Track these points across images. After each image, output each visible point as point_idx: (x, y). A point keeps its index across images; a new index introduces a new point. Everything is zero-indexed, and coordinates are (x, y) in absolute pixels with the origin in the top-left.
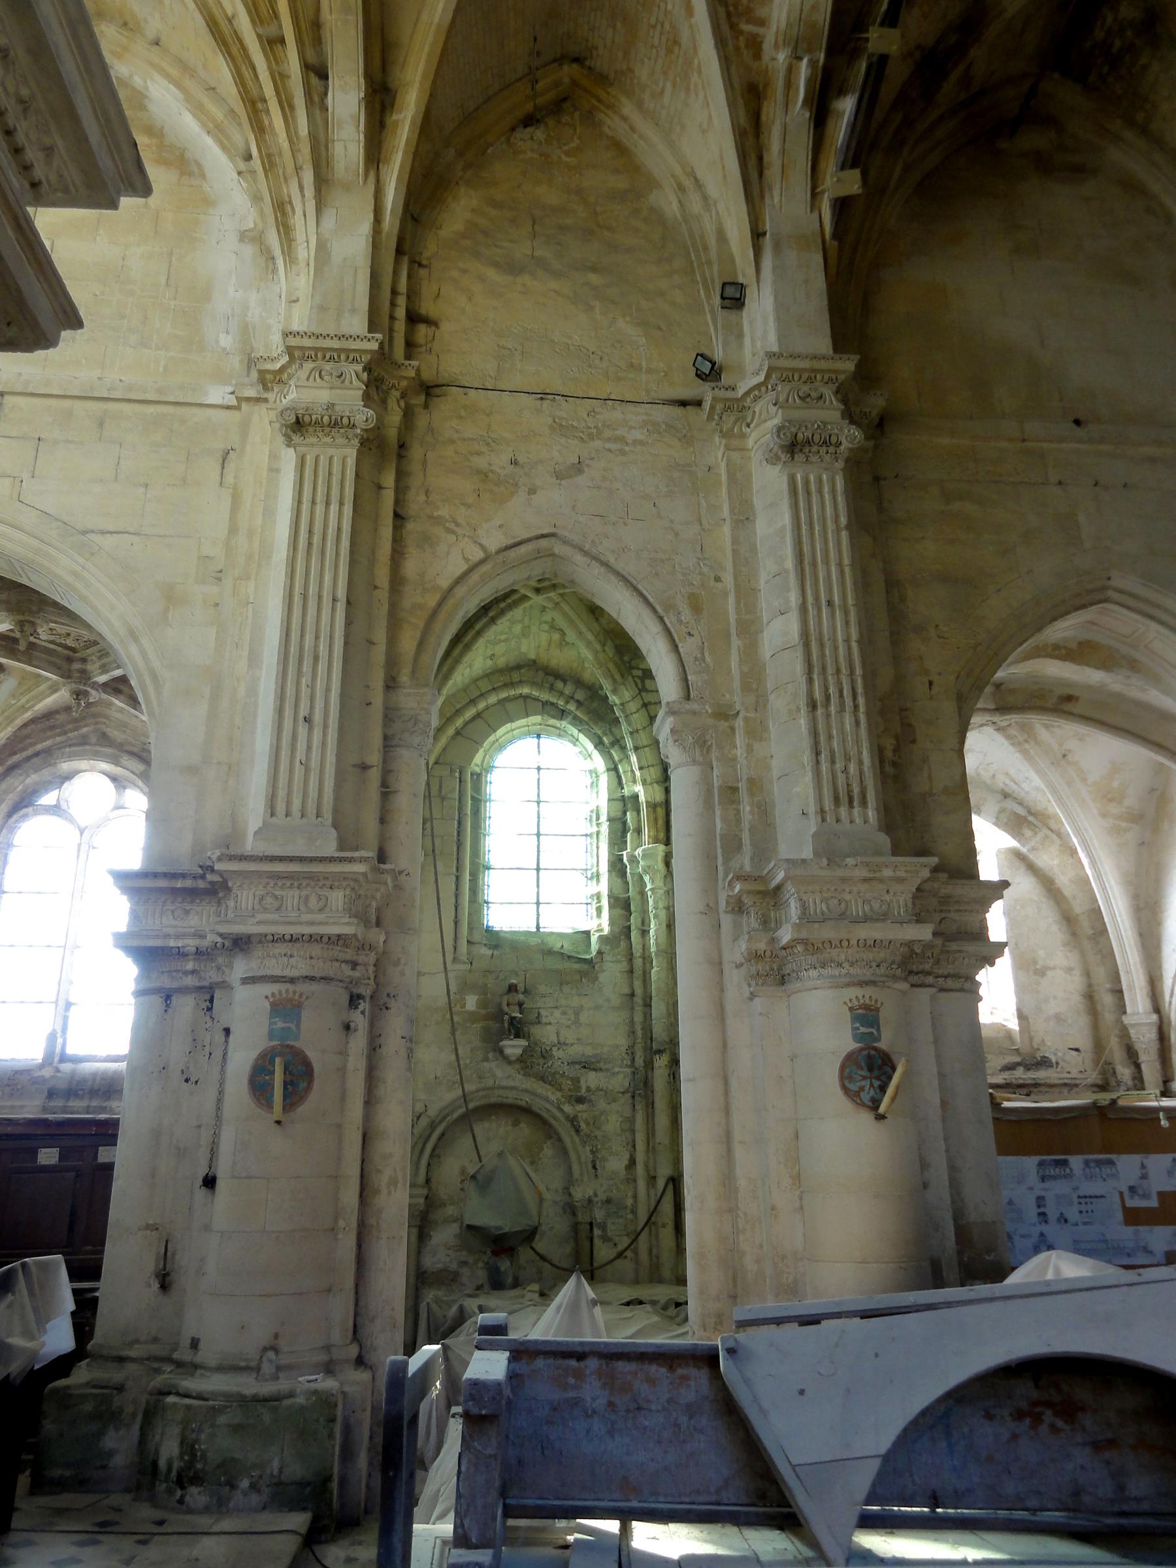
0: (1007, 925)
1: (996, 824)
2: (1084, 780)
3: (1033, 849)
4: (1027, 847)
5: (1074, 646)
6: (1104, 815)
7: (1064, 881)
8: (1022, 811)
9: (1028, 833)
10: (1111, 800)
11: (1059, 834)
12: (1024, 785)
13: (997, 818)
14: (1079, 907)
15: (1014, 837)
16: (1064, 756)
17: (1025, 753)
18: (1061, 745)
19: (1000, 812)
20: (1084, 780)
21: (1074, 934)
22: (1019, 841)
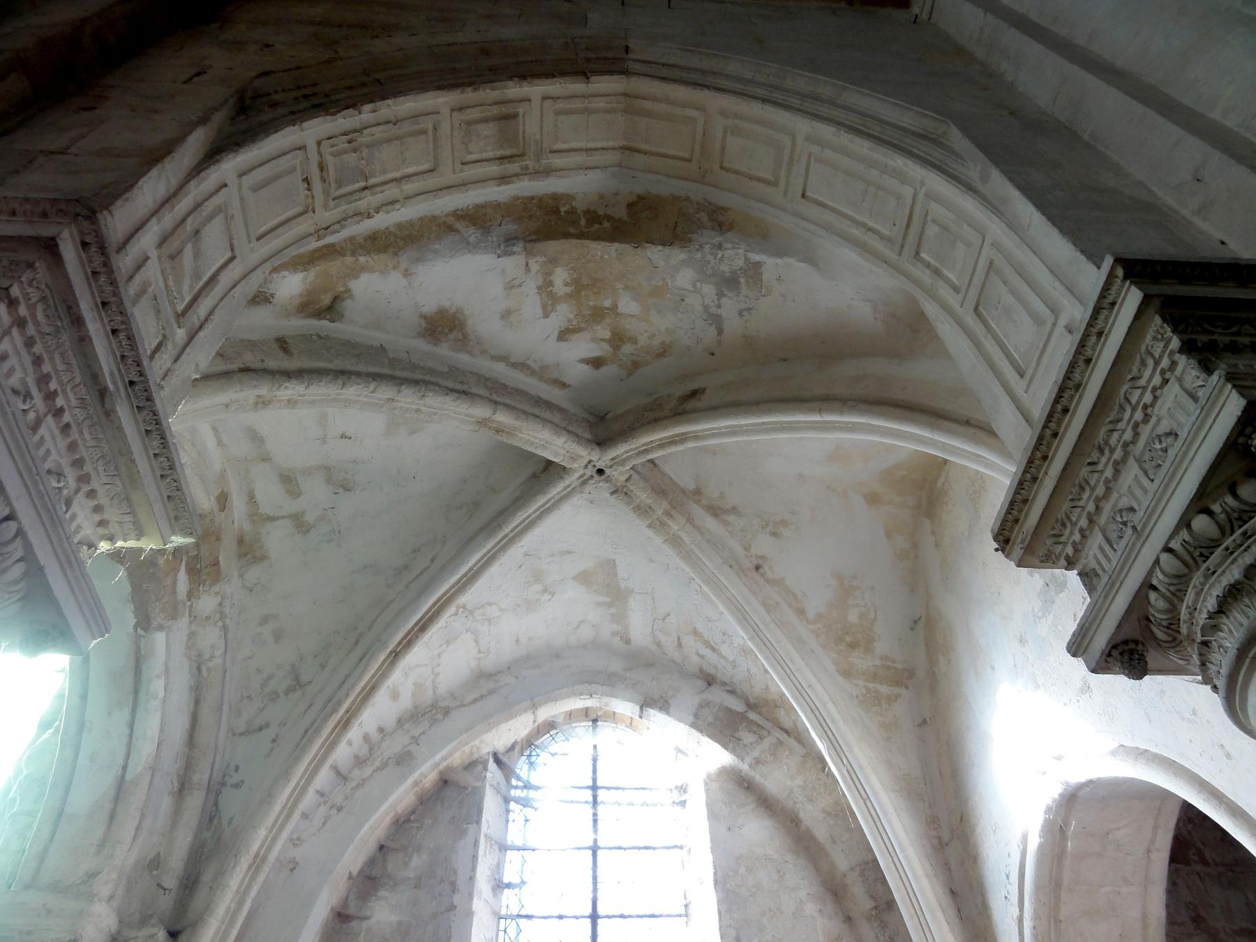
0: (720, 902)
1: (694, 726)
2: (801, 612)
3: (758, 761)
4: (748, 760)
5: (621, 213)
6: (847, 674)
7: (812, 815)
8: (738, 706)
9: (748, 737)
10: (853, 646)
11: (800, 737)
12: (725, 650)
13: (696, 716)
14: (842, 862)
15: (725, 747)
16: (758, 568)
17: (675, 542)
18: (747, 549)
19: (701, 706)
20: (801, 612)
21: (848, 919)
22: (733, 751)
